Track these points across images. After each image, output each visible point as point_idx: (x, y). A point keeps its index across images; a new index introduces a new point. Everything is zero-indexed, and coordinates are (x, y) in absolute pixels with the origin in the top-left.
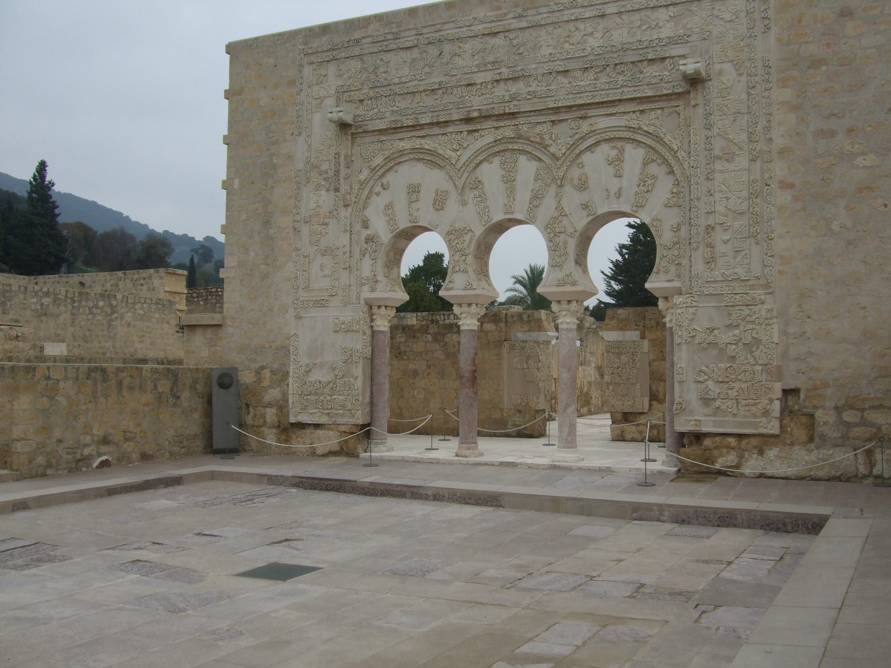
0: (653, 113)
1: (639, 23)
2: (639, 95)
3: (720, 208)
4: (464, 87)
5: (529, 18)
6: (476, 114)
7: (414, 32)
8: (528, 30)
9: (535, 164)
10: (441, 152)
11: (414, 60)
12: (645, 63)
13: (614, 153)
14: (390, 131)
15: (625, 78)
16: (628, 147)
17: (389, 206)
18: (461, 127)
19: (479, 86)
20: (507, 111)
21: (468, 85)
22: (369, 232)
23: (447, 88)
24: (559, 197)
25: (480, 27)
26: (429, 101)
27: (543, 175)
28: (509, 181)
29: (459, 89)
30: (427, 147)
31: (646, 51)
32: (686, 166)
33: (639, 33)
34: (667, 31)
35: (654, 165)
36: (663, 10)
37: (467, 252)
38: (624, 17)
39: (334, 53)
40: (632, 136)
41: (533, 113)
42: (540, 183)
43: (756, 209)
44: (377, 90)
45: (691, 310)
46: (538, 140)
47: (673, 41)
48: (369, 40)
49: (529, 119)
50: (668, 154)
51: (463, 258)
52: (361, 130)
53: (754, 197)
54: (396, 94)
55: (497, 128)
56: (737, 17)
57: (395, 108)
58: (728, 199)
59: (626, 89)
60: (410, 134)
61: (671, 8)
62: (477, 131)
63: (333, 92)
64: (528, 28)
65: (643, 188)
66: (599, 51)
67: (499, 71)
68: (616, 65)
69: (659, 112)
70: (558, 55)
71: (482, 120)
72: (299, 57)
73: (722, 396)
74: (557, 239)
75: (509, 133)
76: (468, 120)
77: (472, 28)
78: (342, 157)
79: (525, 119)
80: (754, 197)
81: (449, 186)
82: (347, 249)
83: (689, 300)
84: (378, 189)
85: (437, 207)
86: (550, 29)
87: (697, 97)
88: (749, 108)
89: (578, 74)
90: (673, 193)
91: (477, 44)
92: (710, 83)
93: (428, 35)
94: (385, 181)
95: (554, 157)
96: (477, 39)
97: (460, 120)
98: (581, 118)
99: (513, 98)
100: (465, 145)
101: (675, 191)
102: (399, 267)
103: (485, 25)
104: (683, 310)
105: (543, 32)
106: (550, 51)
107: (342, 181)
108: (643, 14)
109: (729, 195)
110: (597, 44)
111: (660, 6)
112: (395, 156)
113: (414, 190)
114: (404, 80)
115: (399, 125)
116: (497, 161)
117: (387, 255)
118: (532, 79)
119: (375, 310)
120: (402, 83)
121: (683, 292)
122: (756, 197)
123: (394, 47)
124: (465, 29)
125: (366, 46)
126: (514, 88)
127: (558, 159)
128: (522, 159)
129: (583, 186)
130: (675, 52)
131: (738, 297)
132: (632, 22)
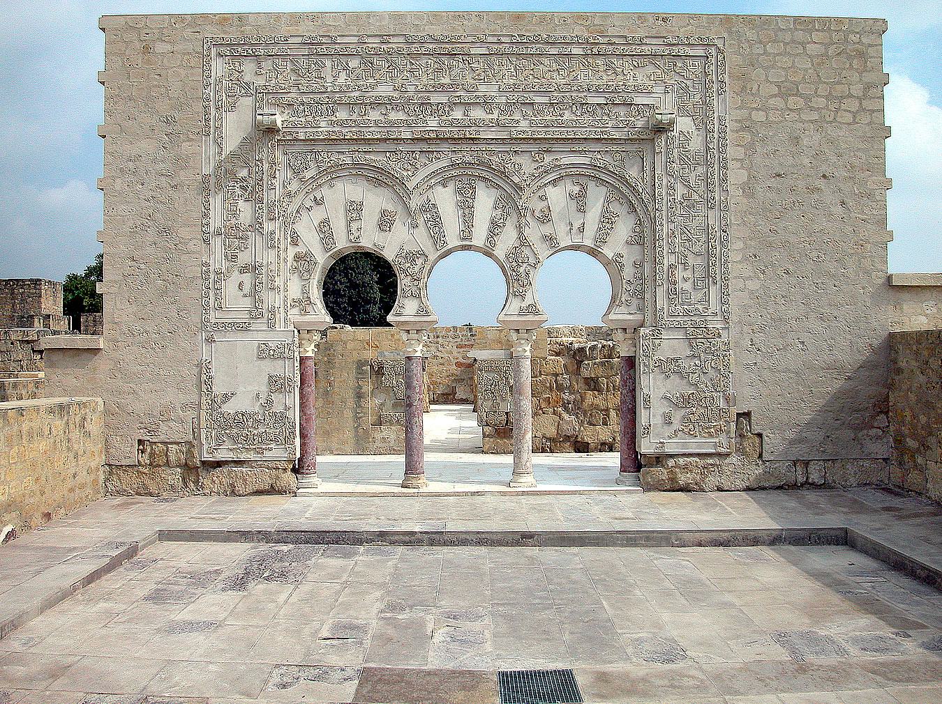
9: (494, 193)
17: (325, 222)
24: (519, 228)
28: (466, 208)
40: (595, 174)
42: (499, 212)
45: (657, 342)
48: (299, 40)
57: (335, 119)
71: (438, 142)
84: (308, 203)
110: (563, 81)
113: (354, 210)
129: (545, 218)
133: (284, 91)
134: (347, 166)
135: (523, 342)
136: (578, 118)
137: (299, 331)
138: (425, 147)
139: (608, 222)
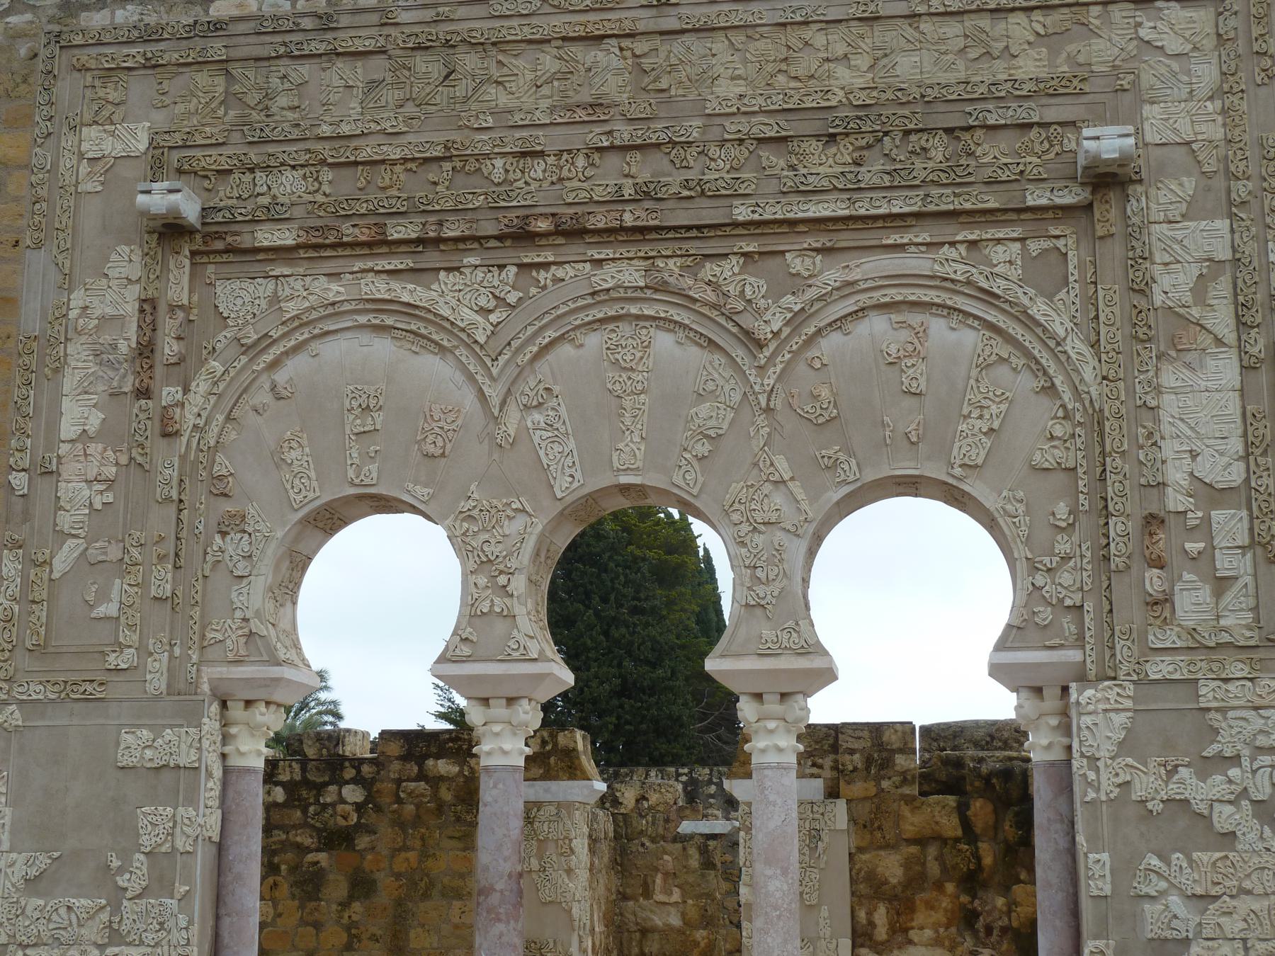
0: (1000, 248)
1: (961, 43)
2: (968, 206)
3: (1177, 475)
4: (510, 159)
5: (684, 11)
6: (543, 225)
7: (374, 18)
8: (686, 38)
10: (446, 312)
11: (373, 85)
12: (979, 133)
13: (905, 335)
14: (302, 253)
15: (930, 164)
16: (938, 327)
18: (498, 254)
19: (551, 160)
20: (628, 220)
21: (524, 154)
22: (228, 506)
23: (464, 159)
25: (557, 20)
26: (416, 186)
27: (721, 382)
29: (499, 163)
30: (406, 298)
31: (980, 106)
32: (1088, 374)
33: (961, 64)
34: (1030, 66)
35: (1003, 372)
36: (1020, 18)
37: (513, 564)
38: (926, 26)
39: (151, 48)
41: (694, 233)
43: (1265, 480)
44: (271, 149)
46: (711, 296)
47: (1047, 91)
49: (685, 245)
50: (1038, 346)
51: (502, 580)
52: (219, 245)
53: (1258, 452)
54: (323, 162)
55: (599, 263)
56: (1195, 48)
57: (320, 198)
58: (1194, 455)
59: (935, 191)
60: (358, 265)
61: (1037, 16)
62: (546, 266)
63: (142, 146)
64: (683, 32)
65: (978, 423)
66: (863, 98)
67: (607, 128)
68: (907, 133)
69: (1018, 245)
70: (761, 101)
71: (561, 240)
72: (44, 53)
73: (1207, 932)
74: (759, 539)
75: (632, 275)
76: (523, 236)
77: (534, 21)
78: (163, 308)
79: (677, 245)
80: (1258, 452)
81: (469, 400)
82: (170, 546)
83: (1112, 695)
84: (262, 397)
85: (431, 449)
86: (738, 38)
87: (1108, 215)
88: (1234, 250)
89: (814, 146)
90: (1052, 438)
91: (548, 61)
92: (1139, 188)
93: (417, 29)
94: (281, 376)
95: (753, 342)
96: (546, 47)
97: (499, 238)
98: (817, 250)
99: (645, 194)
100: (512, 298)
101: (1058, 431)
102: (294, 603)
103: (568, 18)
104: (1099, 719)
105: (719, 43)
106: (739, 90)
107: (159, 371)
108: (969, 22)
109: (1198, 445)
110: (860, 82)
111: (1013, 10)
112: (315, 315)
114: (346, 129)
115: (331, 240)
116: (593, 341)
117: (277, 567)
118: (693, 151)
119: (236, 711)
120: (339, 137)
121: (1092, 674)
122: (1264, 453)
123: (322, 48)
124: (515, 22)
125: (242, 40)
126: (643, 169)
127: (760, 345)
128: (664, 341)
130: (1051, 115)
131: (1230, 686)
132: (943, 40)
133: (209, 142)
134: (347, 307)
135: (772, 725)
136: (898, 166)
137: (224, 705)
138: (531, 257)
139: (981, 417)
